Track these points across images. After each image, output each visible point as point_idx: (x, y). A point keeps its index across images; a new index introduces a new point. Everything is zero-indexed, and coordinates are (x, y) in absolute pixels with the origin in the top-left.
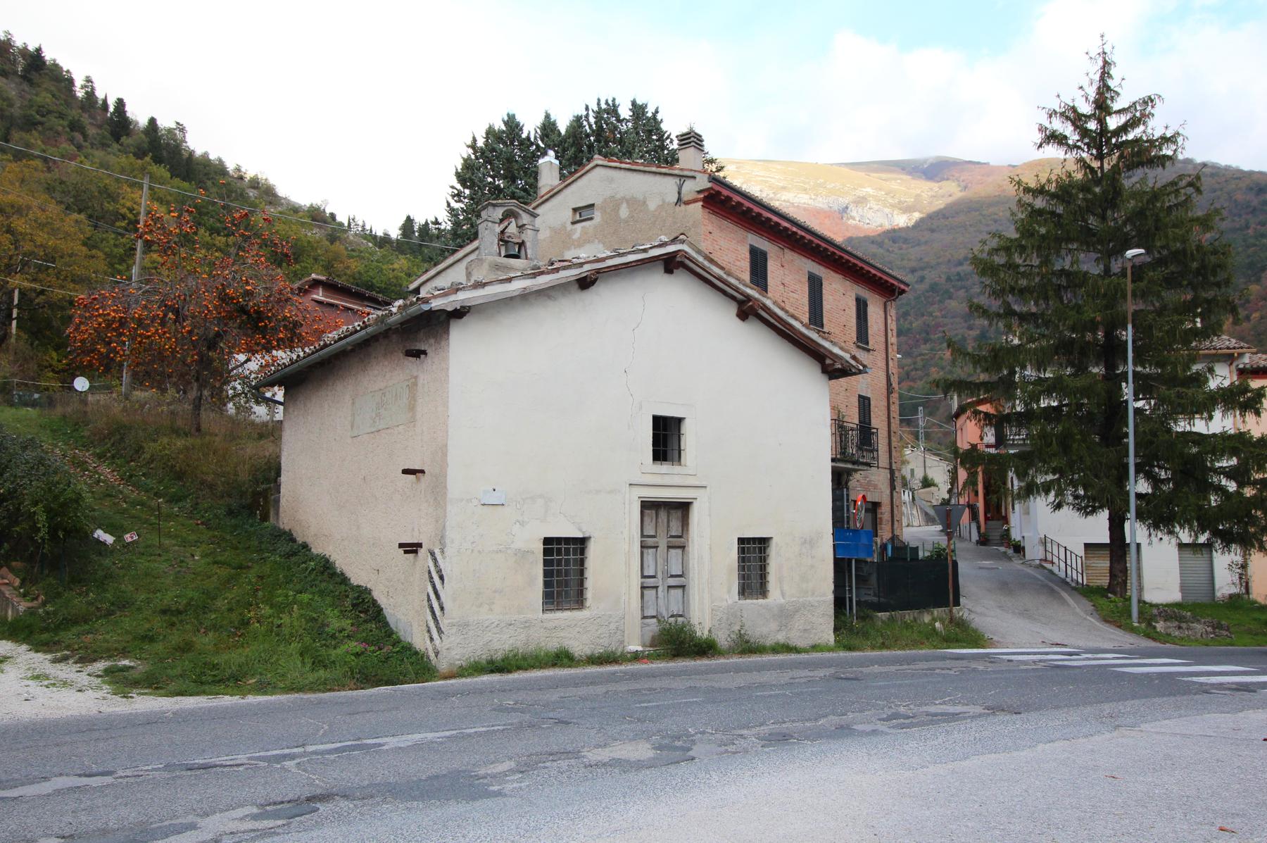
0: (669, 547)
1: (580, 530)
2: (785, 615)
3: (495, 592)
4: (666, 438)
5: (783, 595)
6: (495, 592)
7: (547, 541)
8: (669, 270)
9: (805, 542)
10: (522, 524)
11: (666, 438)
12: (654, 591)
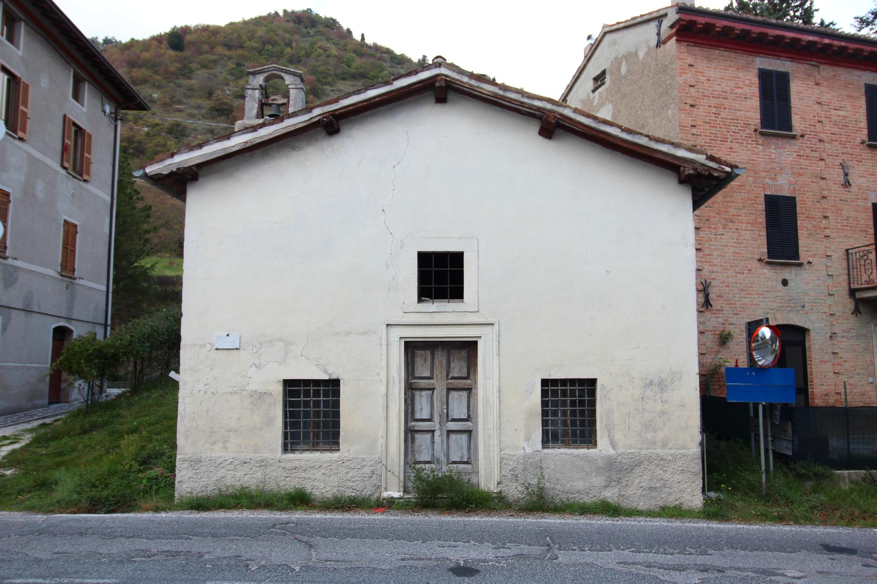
0: (449, 390)
1: (325, 372)
2: (617, 469)
3: (229, 431)
4: (440, 276)
5: (613, 445)
6: (229, 431)
7: (287, 383)
8: (441, 99)
9: (651, 383)
10: (258, 366)
11: (440, 276)
12: (428, 436)
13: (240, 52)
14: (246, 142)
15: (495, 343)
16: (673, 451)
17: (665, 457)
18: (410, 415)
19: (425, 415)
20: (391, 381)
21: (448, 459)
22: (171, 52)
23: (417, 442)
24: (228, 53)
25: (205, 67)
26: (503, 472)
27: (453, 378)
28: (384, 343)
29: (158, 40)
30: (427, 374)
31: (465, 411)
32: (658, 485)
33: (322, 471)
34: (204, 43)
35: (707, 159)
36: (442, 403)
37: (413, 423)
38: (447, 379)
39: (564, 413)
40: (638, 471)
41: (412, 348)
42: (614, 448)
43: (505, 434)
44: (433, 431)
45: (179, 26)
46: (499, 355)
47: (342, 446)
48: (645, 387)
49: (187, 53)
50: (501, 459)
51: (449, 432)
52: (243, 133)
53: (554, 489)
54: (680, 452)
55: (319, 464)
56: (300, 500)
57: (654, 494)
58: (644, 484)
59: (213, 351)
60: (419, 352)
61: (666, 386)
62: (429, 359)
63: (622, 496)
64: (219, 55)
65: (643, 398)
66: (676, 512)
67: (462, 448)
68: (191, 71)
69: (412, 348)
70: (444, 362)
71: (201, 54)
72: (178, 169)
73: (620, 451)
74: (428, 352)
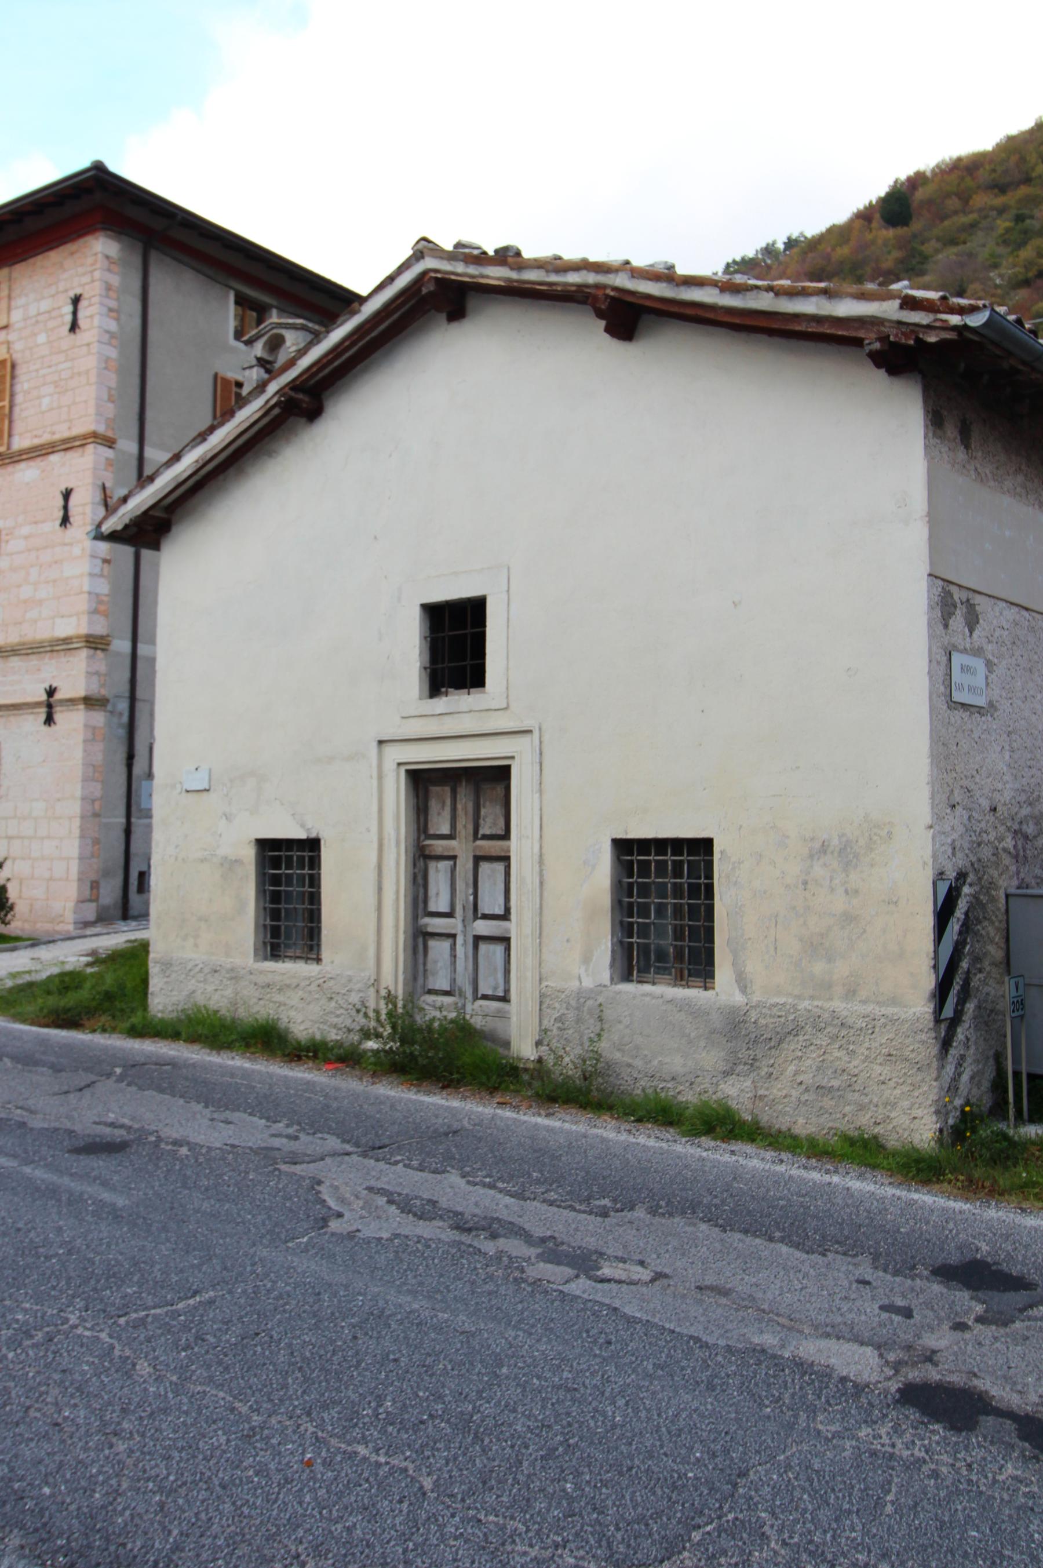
0: (478, 859)
1: (303, 826)
2: (748, 1038)
3: (200, 919)
4: (456, 643)
5: (743, 983)
6: (200, 919)
7: (264, 845)
8: (457, 313)
9: (824, 849)
10: (228, 817)
11: (456, 643)
12: (446, 944)
13: (1023, 190)
14: (197, 461)
15: (538, 768)
16: (869, 1008)
17: (850, 1021)
18: (421, 905)
19: (443, 907)
20: (386, 842)
21: (476, 989)
22: (890, 233)
23: (431, 954)
24: (999, 201)
25: (953, 242)
26: (545, 1022)
27: (485, 837)
28: (375, 775)
29: (864, 216)
30: (445, 830)
31: (501, 900)
32: (836, 1083)
33: (300, 993)
34: (948, 195)
35: (901, 307)
36: (467, 884)
37: (427, 920)
38: (476, 836)
39: (661, 910)
40: (792, 1046)
41: (422, 781)
42: (744, 990)
43: (555, 946)
44: (453, 936)
45: (903, 177)
46: (541, 791)
47: (325, 954)
48: (811, 856)
49: (916, 226)
50: (542, 996)
51: (478, 939)
52: (193, 447)
53: (629, 1065)
54: (883, 1011)
55: (295, 982)
56: (268, 1039)
57: (827, 1103)
58: (807, 1078)
59: (184, 794)
60: (434, 789)
61: (856, 856)
62: (448, 802)
63: (762, 1098)
64: (980, 210)
65: (805, 883)
66: (864, 1150)
67: (495, 969)
68: (925, 258)
69: (422, 781)
70: (470, 806)
71: (943, 218)
72: (131, 520)
73: (756, 998)
74: (447, 789)
